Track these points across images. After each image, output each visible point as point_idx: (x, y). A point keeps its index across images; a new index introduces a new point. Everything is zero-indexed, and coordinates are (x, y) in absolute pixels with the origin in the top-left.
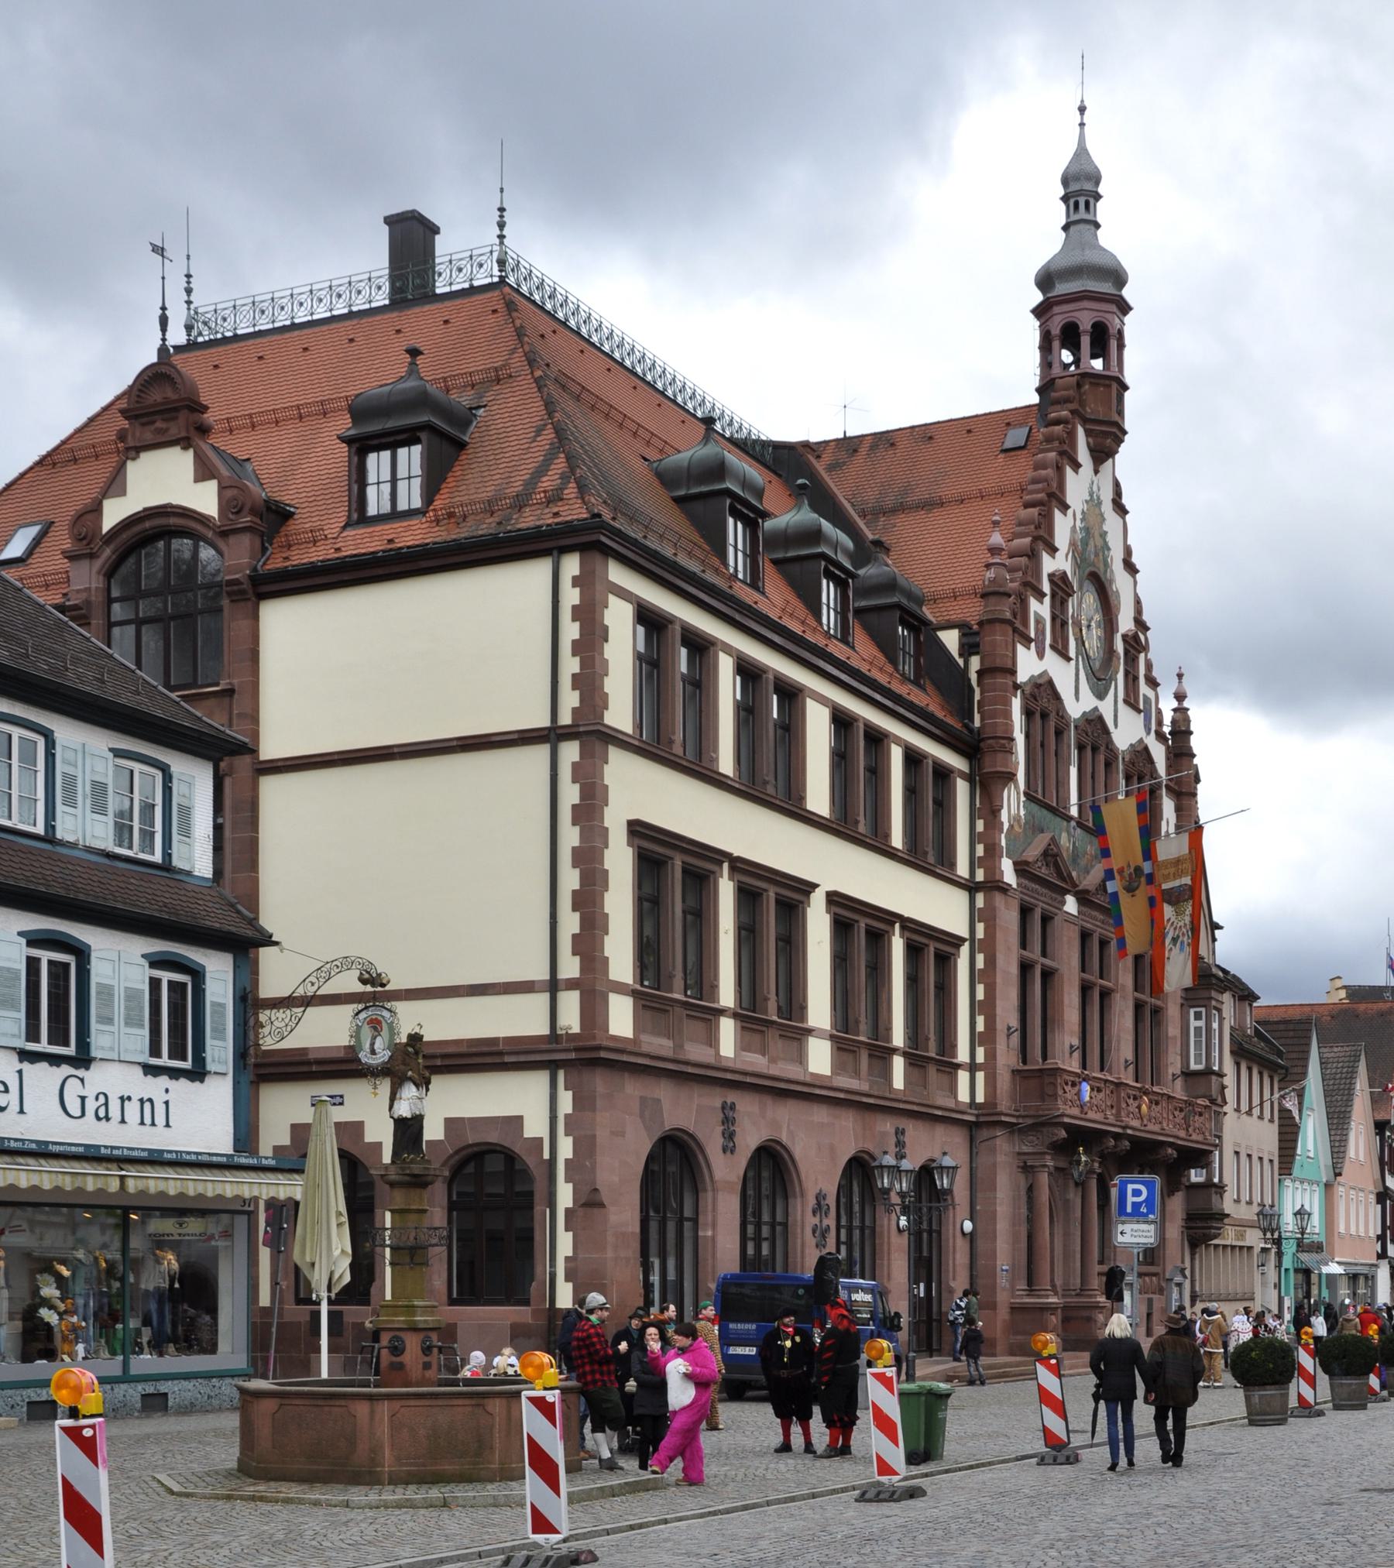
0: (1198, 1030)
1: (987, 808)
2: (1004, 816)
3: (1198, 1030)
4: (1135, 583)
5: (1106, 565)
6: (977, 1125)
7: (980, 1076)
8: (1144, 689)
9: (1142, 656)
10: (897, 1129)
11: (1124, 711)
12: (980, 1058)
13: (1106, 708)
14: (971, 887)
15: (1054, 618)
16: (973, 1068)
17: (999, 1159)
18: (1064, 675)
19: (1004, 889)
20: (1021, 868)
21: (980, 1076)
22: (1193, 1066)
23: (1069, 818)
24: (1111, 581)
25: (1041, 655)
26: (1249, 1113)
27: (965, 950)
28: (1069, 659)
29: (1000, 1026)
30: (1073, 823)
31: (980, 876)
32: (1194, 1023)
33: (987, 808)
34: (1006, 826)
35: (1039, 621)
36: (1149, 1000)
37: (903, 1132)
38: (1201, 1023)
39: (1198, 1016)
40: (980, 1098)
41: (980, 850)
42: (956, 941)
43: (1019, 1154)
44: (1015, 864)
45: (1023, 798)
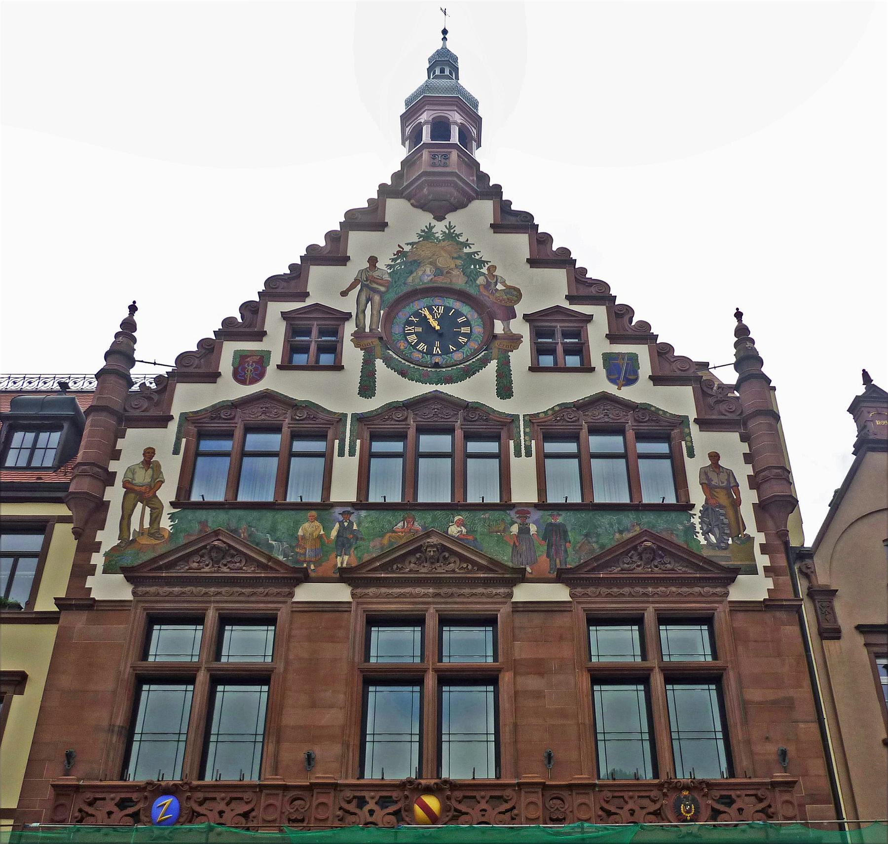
20: (132, 575)
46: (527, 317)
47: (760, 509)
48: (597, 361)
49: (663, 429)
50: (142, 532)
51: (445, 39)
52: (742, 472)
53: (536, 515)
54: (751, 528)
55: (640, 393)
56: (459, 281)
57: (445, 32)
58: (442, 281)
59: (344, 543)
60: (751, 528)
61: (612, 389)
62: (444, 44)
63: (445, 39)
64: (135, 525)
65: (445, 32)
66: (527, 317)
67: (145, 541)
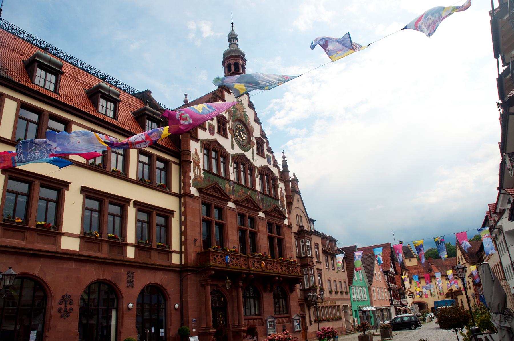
0: (303, 245)
1: (184, 172)
2: (192, 174)
3: (303, 245)
4: (261, 127)
5: (246, 119)
6: (181, 270)
7: (183, 255)
8: (266, 153)
9: (265, 146)
10: (128, 273)
11: (257, 157)
12: (183, 250)
13: (248, 155)
14: (179, 196)
15: (219, 128)
16: (180, 253)
17: (189, 282)
18: (226, 143)
19: (192, 196)
20: (200, 190)
21: (183, 255)
22: (303, 256)
23: (230, 180)
24: (249, 124)
25: (212, 133)
26: (344, 271)
27: (177, 215)
28: (227, 138)
29: (189, 238)
30: (231, 182)
31: (182, 192)
32: (301, 244)
33: (184, 172)
34: (192, 177)
35: (210, 125)
36: (276, 235)
37: (133, 273)
38: (303, 244)
39: (302, 242)
40: (183, 263)
41: (182, 185)
42: (172, 212)
43: (200, 281)
44: (198, 189)
45: (202, 171)
46: (256, 138)
47: (287, 203)
48: (266, 156)
49: (274, 179)
50: (198, 176)
51: (232, 26)
52: (285, 194)
53: (260, 195)
54: (286, 208)
55: (271, 167)
56: (244, 120)
57: (232, 24)
58: (241, 118)
59: (233, 192)
60: (286, 208)
61: (268, 164)
62: (232, 29)
63: (232, 26)
64: (196, 174)
65: (232, 24)
66: (256, 138)
67: (199, 179)
